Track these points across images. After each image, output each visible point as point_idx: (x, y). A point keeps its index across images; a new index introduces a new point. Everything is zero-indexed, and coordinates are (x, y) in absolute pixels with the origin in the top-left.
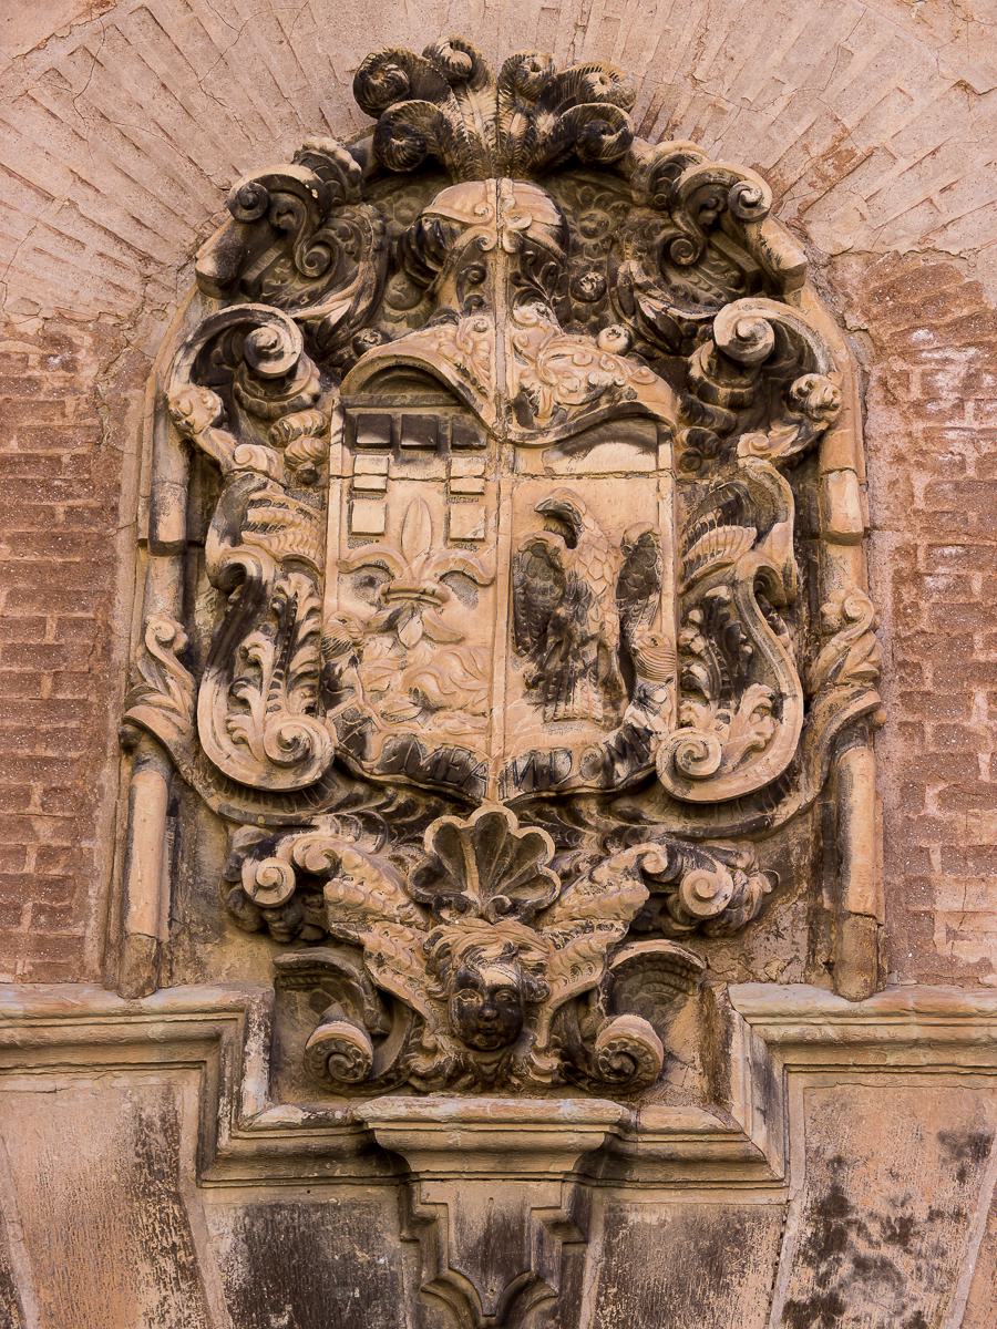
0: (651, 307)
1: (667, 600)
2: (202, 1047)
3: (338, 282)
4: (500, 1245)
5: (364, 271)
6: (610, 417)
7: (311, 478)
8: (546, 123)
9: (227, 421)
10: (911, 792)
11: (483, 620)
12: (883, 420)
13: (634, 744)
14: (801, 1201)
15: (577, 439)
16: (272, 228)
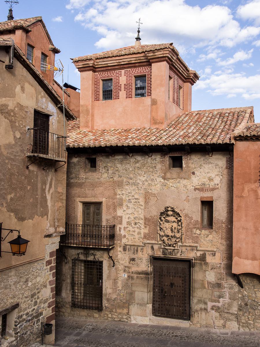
0: (176, 217)
1: (176, 229)
2: (160, 244)
3: (165, 215)
4: (170, 252)
5: (166, 214)
6: (174, 222)
7: (163, 223)
8: (172, 209)
9: (161, 221)
10: (185, 236)
11: (170, 229)
12: (185, 221)
13: (175, 235)
14: (181, 251)
15: (173, 223)
16: (162, 214)
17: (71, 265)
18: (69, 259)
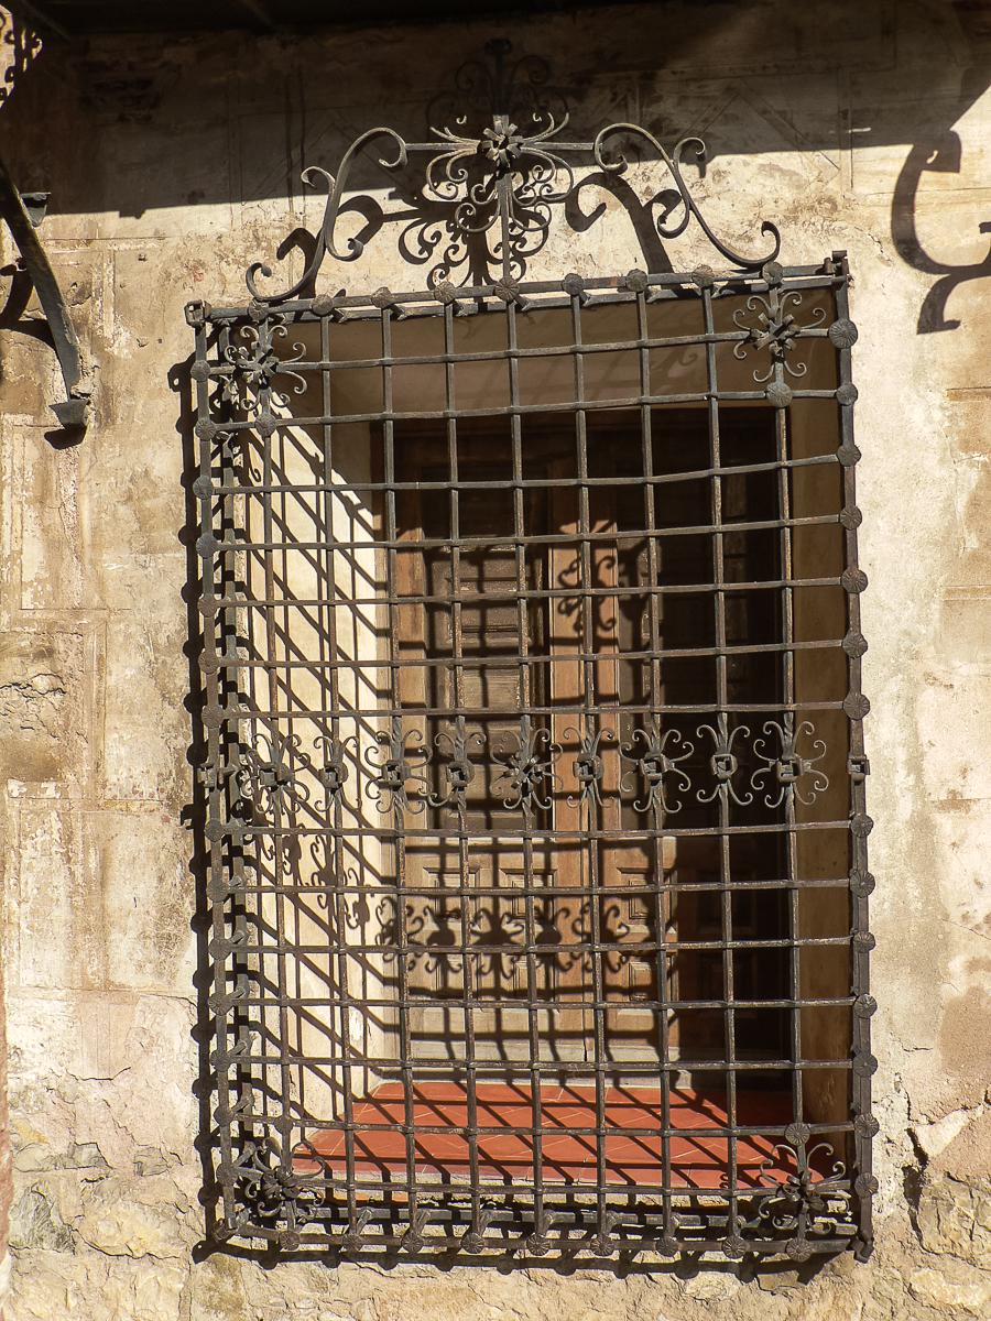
17: (166, 461)
18: (121, 340)
